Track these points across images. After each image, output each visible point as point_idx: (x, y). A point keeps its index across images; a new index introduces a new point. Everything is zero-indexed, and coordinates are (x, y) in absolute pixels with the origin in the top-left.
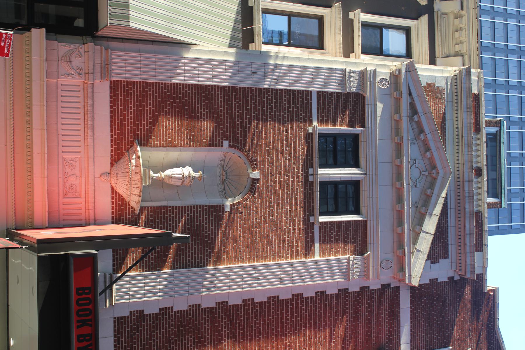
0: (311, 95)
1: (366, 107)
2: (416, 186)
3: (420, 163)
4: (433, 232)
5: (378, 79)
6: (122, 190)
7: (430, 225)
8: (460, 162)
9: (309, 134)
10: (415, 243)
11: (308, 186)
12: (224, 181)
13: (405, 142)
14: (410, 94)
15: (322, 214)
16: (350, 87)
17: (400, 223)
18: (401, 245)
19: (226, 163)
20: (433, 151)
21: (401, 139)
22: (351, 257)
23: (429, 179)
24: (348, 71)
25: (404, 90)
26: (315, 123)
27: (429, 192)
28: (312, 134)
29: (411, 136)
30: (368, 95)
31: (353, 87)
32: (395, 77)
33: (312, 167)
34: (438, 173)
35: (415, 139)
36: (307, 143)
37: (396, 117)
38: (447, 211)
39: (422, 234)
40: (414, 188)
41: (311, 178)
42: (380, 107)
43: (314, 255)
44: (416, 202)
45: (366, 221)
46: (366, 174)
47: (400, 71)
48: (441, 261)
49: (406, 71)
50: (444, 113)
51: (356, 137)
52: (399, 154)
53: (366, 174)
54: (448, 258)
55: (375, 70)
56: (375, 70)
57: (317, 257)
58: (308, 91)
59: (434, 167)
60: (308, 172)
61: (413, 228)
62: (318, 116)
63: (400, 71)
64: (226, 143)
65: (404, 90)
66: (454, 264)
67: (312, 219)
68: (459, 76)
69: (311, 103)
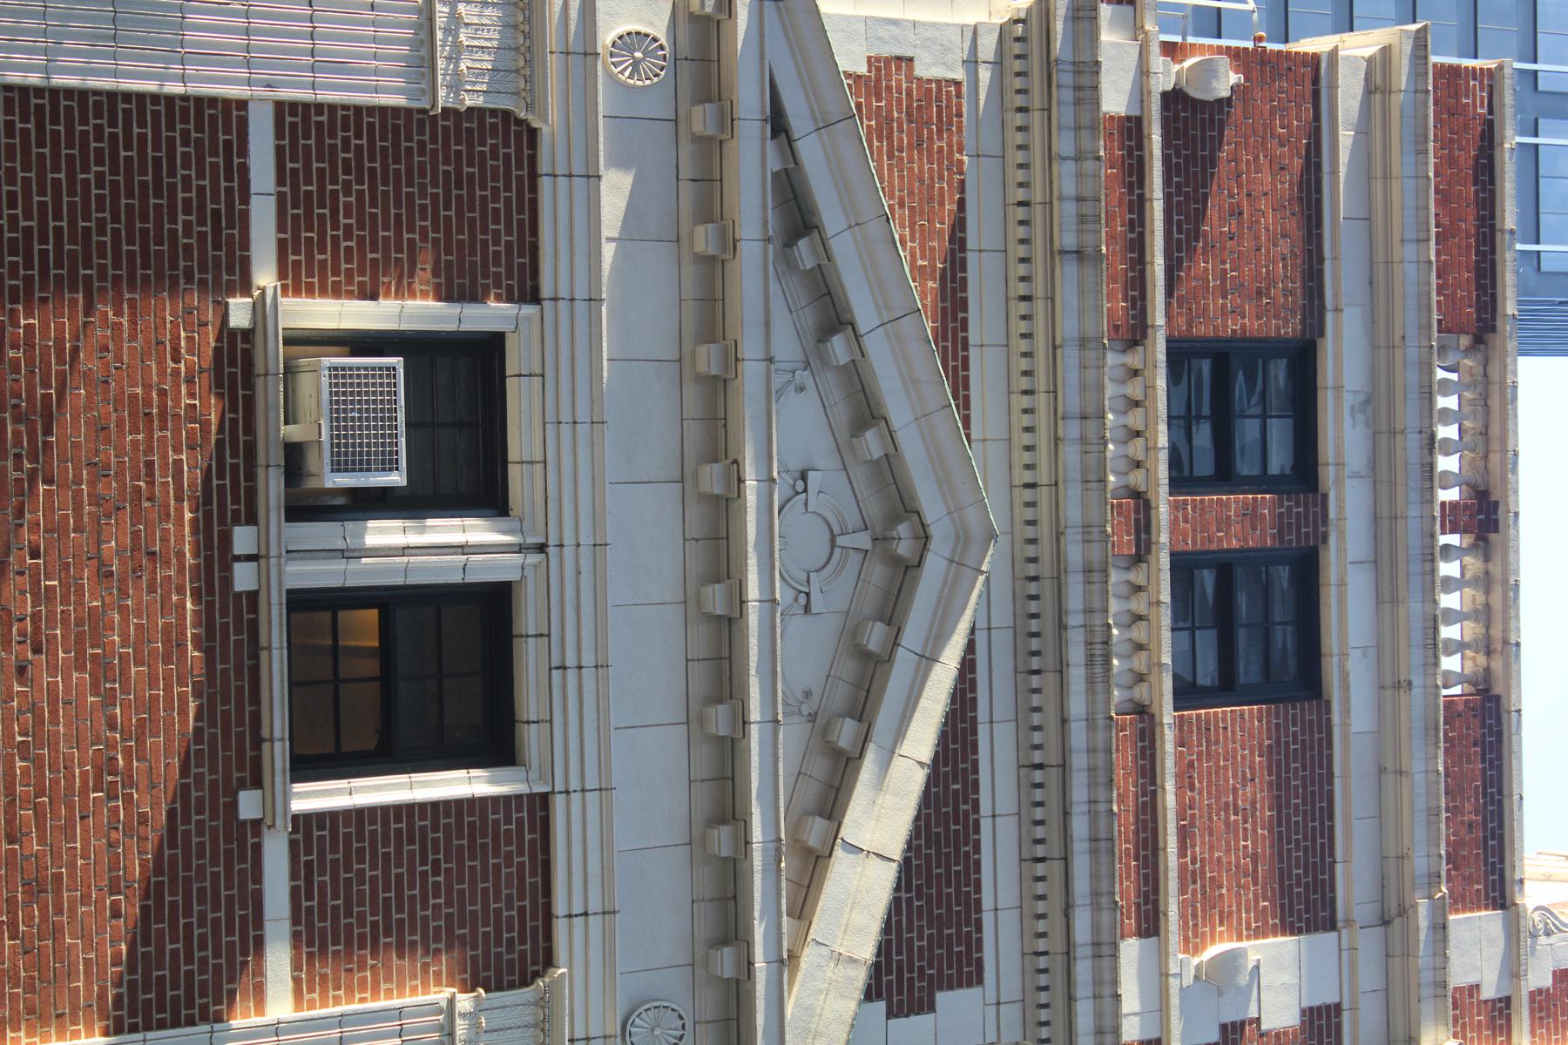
0: (243, 124)
1: (545, 184)
2: (807, 609)
3: (833, 492)
4: (896, 849)
5: (607, 36)
7: (884, 811)
8: (1043, 476)
9: (233, 333)
10: (802, 909)
11: (229, 621)
13: (751, 372)
14: (778, 124)
15: (307, 766)
16: (455, 86)
17: (725, 806)
18: (730, 928)
20: (896, 423)
21: (732, 359)
22: (465, 1002)
23: (878, 572)
25: (749, 100)
26: (265, 277)
27: (875, 636)
28: (247, 334)
29: (787, 346)
30: (551, 123)
33: (252, 519)
34: (923, 538)
35: (807, 365)
36: (219, 384)
38: (975, 732)
39: (841, 865)
40: (799, 622)
41: (244, 578)
43: (259, 991)
44: (808, 694)
45: (544, 799)
46: (541, 548)
48: (942, 997)
50: (959, 224)
51: (487, 351)
52: (718, 444)
53: (541, 548)
54: (980, 982)
57: (280, 1006)
58: (227, 102)
59: (903, 507)
61: (795, 830)
62: (282, 245)
65: (749, 100)
66: (1011, 1014)
67: (249, 805)
68: (1034, 22)
69: (244, 170)
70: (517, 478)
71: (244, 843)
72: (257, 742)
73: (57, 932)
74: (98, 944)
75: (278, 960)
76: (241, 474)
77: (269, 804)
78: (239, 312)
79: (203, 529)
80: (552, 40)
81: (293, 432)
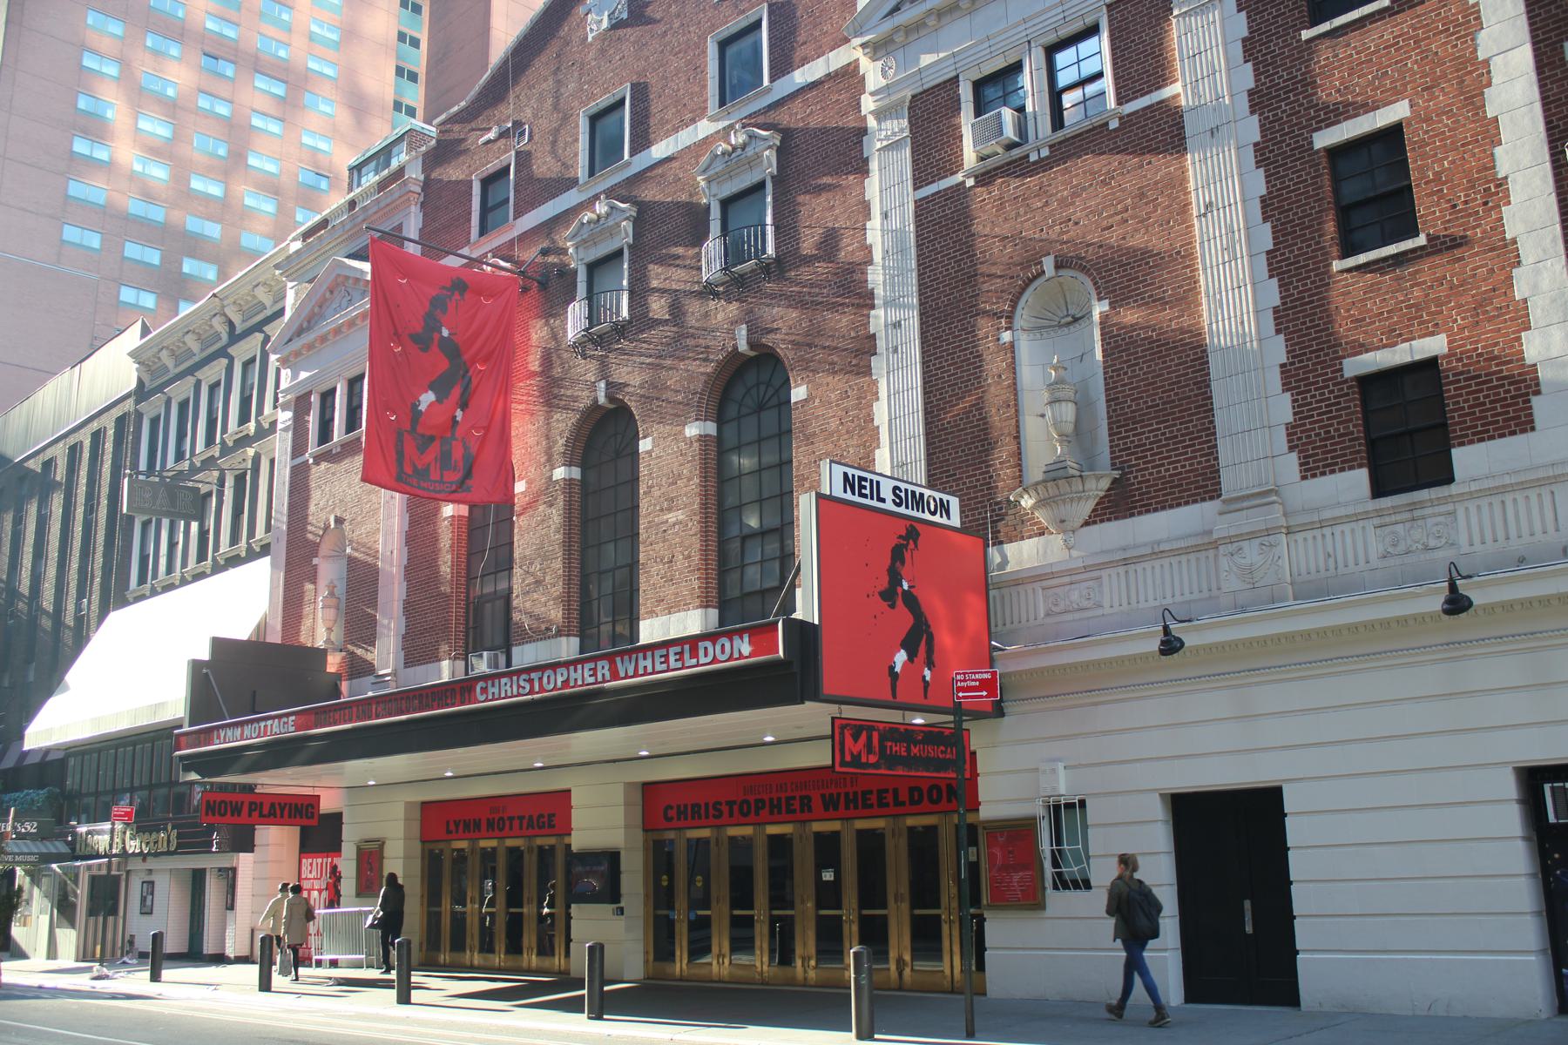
5: (884, 82)
6: (1087, 508)
12: (1076, 320)
14: (896, 9)
16: (902, 130)
19: (1046, 323)
22: (1176, 12)
24: (879, 145)
25: (888, 25)
26: (959, 177)
30: (908, 94)
31: (899, 126)
32: (876, 49)
37: (931, 22)
42: (926, 60)
47: (863, 46)
49: (861, 35)
51: (978, 86)
55: (872, 94)
56: (872, 94)
60: (1035, 163)
63: (863, 46)
64: (1006, 336)
65: (888, 25)
67: (1114, 124)
70: (1011, 61)
71: (1126, 121)
72: (1094, 128)
73: (1156, 183)
74: (1160, 166)
75: (1167, 92)
76: (1010, 166)
77: (1112, 117)
78: (970, 182)
79: (1031, 173)
80: (887, 101)
81: (1000, 150)
